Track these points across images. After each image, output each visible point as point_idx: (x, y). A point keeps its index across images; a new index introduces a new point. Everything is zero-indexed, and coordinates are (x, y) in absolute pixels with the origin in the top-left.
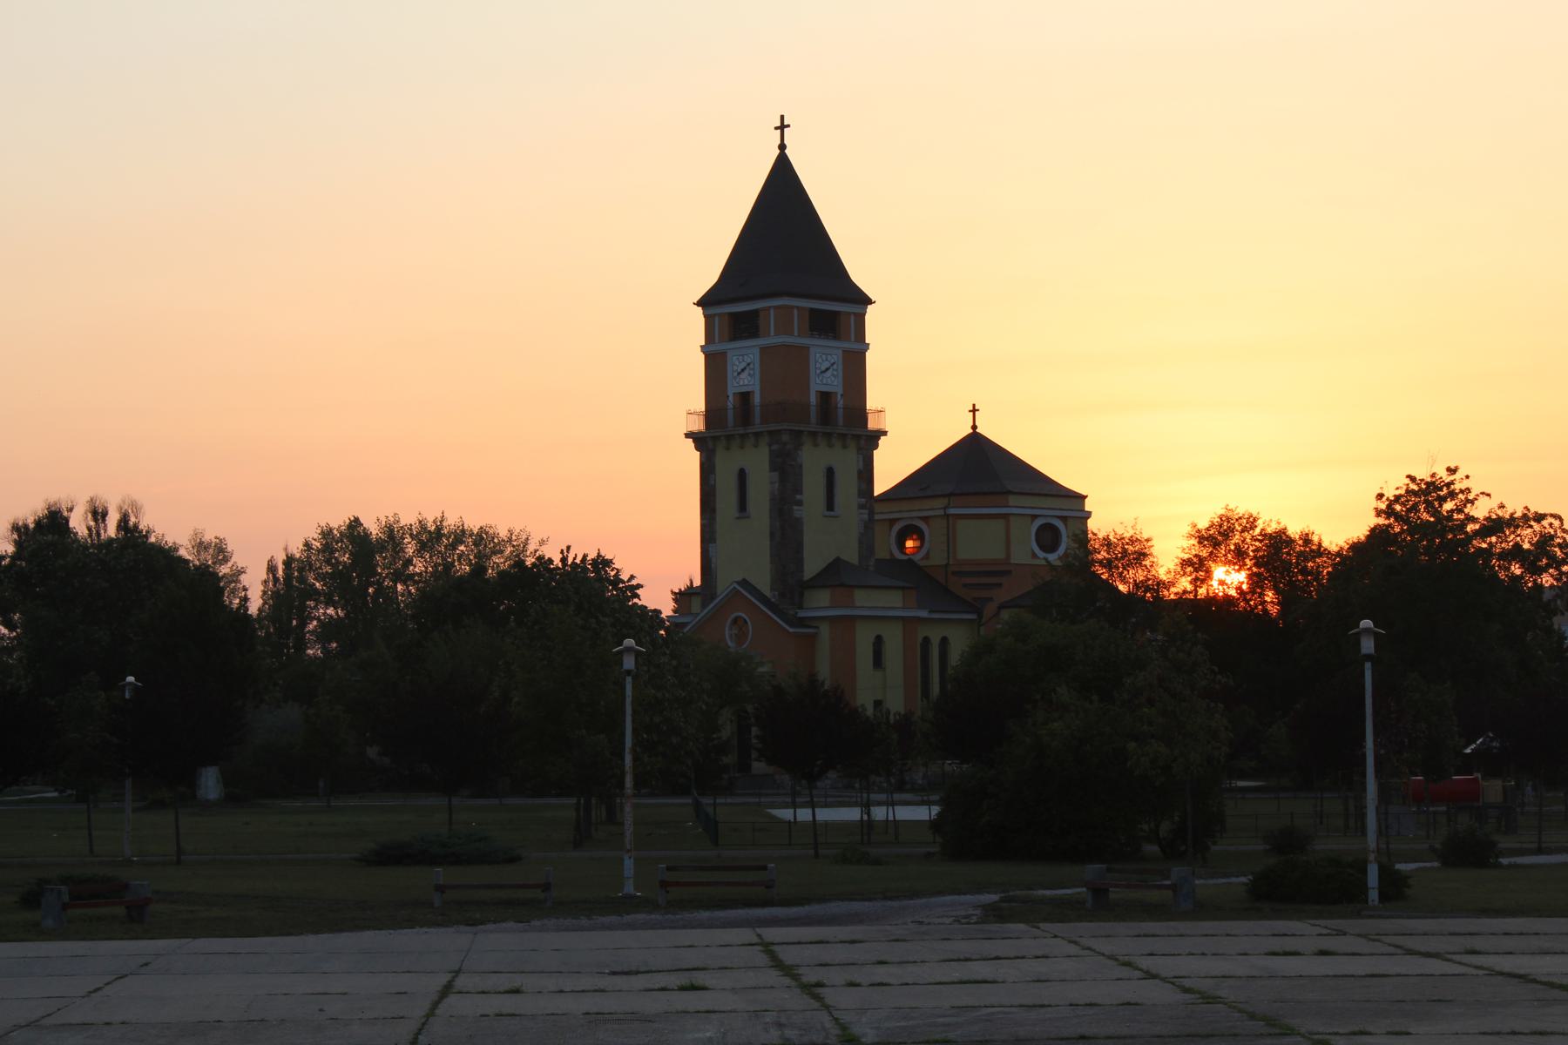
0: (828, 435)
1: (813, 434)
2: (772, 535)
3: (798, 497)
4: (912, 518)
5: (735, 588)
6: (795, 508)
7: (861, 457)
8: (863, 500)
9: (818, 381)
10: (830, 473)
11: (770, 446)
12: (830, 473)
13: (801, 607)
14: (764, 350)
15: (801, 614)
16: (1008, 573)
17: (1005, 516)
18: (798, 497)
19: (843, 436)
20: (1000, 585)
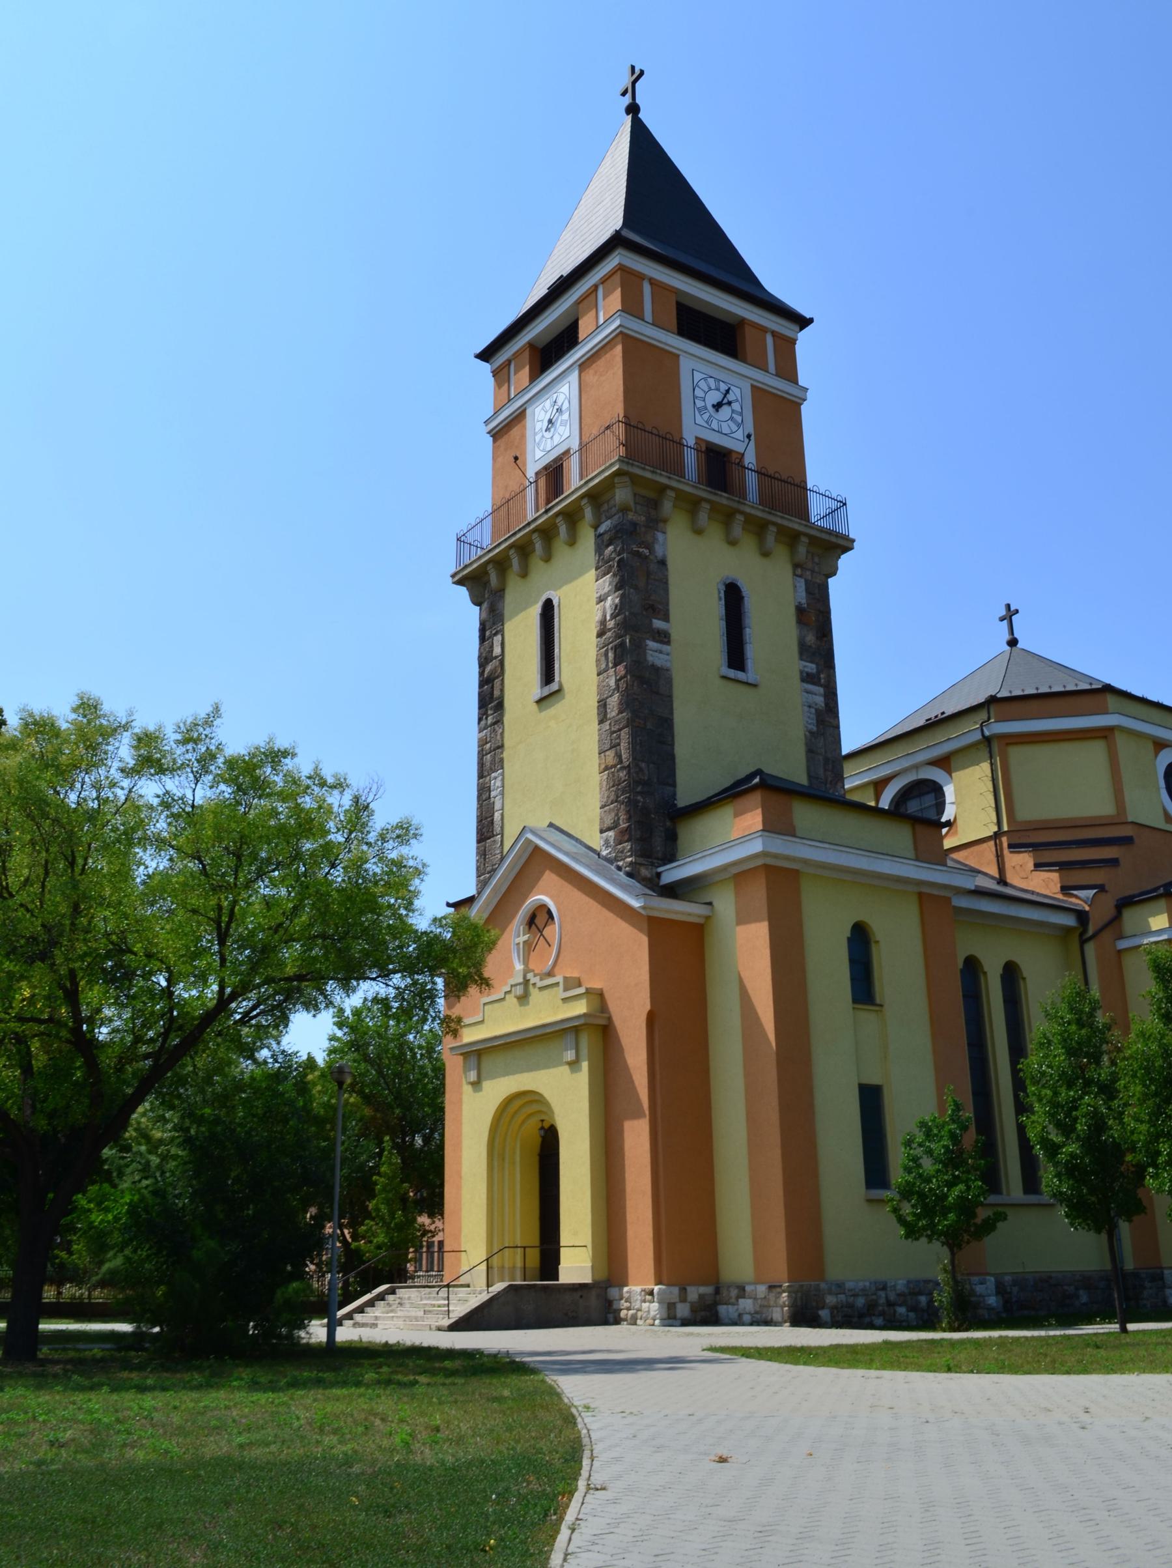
0: (726, 517)
1: (692, 505)
2: (603, 705)
3: (658, 624)
4: (916, 767)
5: (529, 841)
6: (651, 644)
7: (801, 584)
8: (814, 666)
9: (699, 420)
10: (733, 596)
11: (596, 528)
12: (733, 596)
13: (670, 857)
14: (584, 365)
15: (673, 874)
16: (1127, 841)
17: (1105, 734)
18: (658, 624)
19: (759, 528)
20: (1114, 862)
